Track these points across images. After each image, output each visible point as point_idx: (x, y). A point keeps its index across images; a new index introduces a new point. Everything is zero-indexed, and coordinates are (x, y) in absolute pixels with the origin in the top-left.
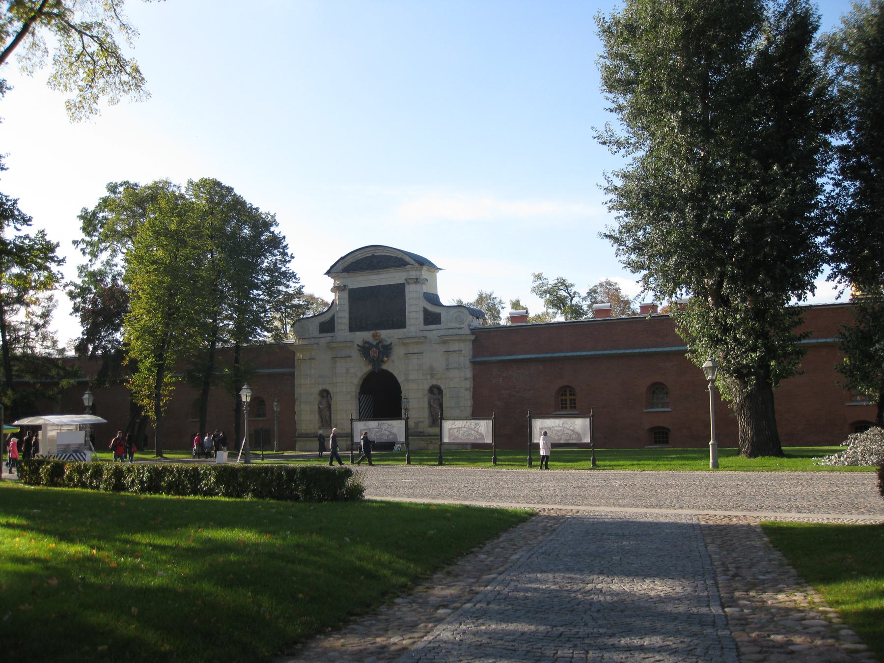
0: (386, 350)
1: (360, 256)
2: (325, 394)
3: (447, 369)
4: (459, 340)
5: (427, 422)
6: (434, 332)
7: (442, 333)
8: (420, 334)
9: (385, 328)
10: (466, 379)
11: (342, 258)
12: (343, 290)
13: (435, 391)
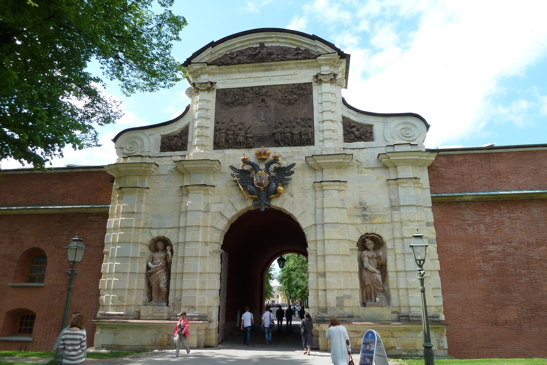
0: (283, 174)
1: (238, 45)
2: (160, 245)
3: (394, 207)
4: (415, 163)
5: (357, 297)
6: (365, 152)
7: (383, 151)
8: (343, 152)
9: (277, 144)
10: (428, 224)
11: (213, 44)
12: (208, 90)
13: (370, 244)
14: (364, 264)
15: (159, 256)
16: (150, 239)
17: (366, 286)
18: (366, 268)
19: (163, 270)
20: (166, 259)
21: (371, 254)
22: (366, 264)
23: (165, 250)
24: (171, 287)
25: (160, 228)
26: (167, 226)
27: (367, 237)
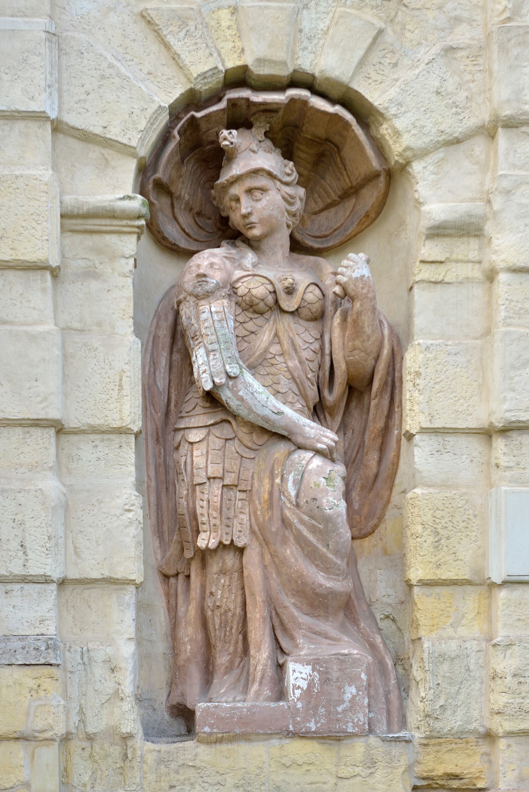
14: (199, 357)
17: (204, 556)
18: (212, 399)
21: (261, 272)
22: (207, 367)
27: (240, 118)
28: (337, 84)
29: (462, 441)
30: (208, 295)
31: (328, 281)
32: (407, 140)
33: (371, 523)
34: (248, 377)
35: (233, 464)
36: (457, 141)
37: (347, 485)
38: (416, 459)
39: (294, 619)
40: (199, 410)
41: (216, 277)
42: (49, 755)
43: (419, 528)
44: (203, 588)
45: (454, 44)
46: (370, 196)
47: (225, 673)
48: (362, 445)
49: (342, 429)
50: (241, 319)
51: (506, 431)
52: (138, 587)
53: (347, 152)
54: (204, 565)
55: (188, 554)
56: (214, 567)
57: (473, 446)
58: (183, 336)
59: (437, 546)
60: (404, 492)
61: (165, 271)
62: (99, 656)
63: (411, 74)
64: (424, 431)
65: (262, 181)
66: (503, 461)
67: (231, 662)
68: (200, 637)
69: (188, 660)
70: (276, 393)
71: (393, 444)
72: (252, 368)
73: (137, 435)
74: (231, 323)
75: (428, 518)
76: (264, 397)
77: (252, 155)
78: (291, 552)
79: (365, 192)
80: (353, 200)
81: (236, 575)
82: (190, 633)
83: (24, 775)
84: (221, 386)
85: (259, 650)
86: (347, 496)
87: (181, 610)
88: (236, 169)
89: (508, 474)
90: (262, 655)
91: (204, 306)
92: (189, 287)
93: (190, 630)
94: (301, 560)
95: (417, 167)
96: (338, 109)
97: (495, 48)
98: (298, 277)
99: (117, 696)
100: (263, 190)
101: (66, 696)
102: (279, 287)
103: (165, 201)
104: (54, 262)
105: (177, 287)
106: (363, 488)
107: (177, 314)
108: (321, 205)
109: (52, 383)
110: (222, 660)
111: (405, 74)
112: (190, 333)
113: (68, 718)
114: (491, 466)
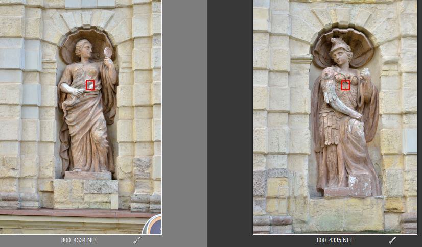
2: (84, 47)
15: (86, 69)
16: (64, 31)
19: (96, 101)
20: (100, 77)
23: (96, 56)
24: (121, 134)
25: (83, 9)
26: (100, 5)
28: (360, 27)
29: (395, 117)
30: (328, 79)
31: (359, 75)
32: (378, 41)
33: (371, 138)
34: (338, 100)
35: (334, 122)
36: (391, 41)
37: (365, 128)
38: (383, 121)
39: (351, 164)
40: (325, 108)
41: (330, 74)
42: (284, 202)
43: (384, 140)
44: (326, 155)
45: (390, 18)
46: (369, 54)
47: (333, 179)
48: (368, 117)
49: (363, 113)
50: (336, 85)
51: (406, 114)
52: (309, 155)
53: (363, 44)
54: (327, 149)
55: (323, 147)
56: (329, 150)
57: (397, 118)
58: (322, 89)
59: (389, 144)
60: (380, 130)
61: (317, 73)
62: (298, 175)
63: (379, 25)
64: (384, 114)
65: (342, 51)
66: (405, 121)
67: (334, 176)
68: (325, 169)
69: (322, 176)
70: (346, 104)
71: (376, 117)
72: (339, 97)
73: (309, 115)
74: (334, 86)
75: (386, 137)
76: (342, 105)
77: (339, 44)
78: (350, 146)
79: (368, 53)
80: (365, 55)
81: (335, 152)
82: (323, 168)
83: (277, 208)
84: (331, 102)
85: (341, 173)
86: (365, 131)
87: (321, 161)
88: (335, 48)
89: (407, 125)
90: (342, 174)
91: (327, 82)
92: (323, 77)
93: (323, 167)
94: (353, 148)
95: (381, 47)
96: (361, 33)
97: (400, 18)
98: (351, 75)
99: (303, 186)
100: (342, 53)
101: (289, 186)
102: (346, 77)
103: (317, 55)
104: (289, 70)
105: (320, 77)
106: (369, 129)
107: (320, 84)
108: (357, 56)
109: (288, 101)
110: (331, 176)
111: (377, 25)
112: (323, 88)
113: (289, 193)
114: (402, 123)
